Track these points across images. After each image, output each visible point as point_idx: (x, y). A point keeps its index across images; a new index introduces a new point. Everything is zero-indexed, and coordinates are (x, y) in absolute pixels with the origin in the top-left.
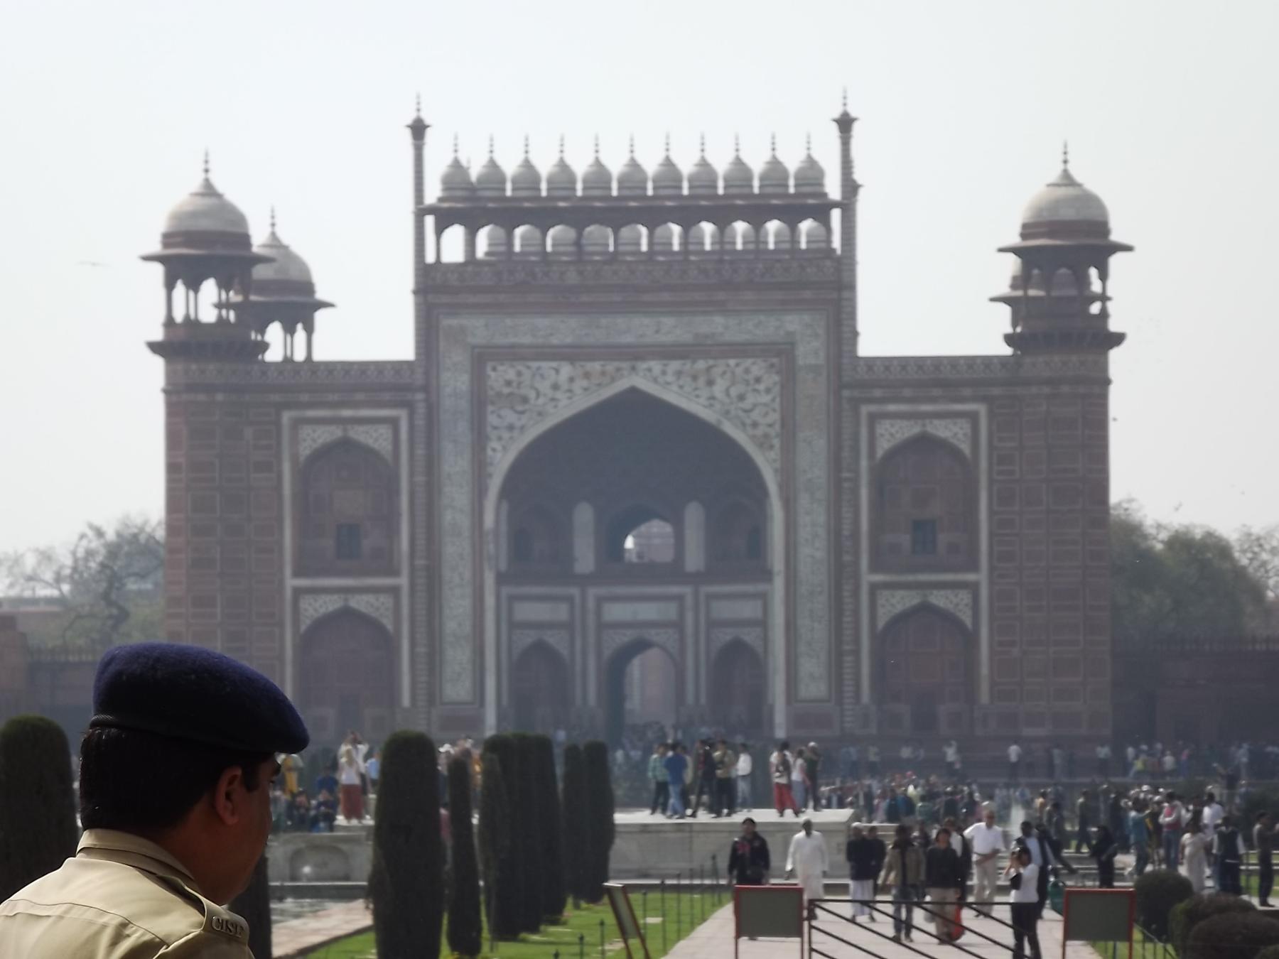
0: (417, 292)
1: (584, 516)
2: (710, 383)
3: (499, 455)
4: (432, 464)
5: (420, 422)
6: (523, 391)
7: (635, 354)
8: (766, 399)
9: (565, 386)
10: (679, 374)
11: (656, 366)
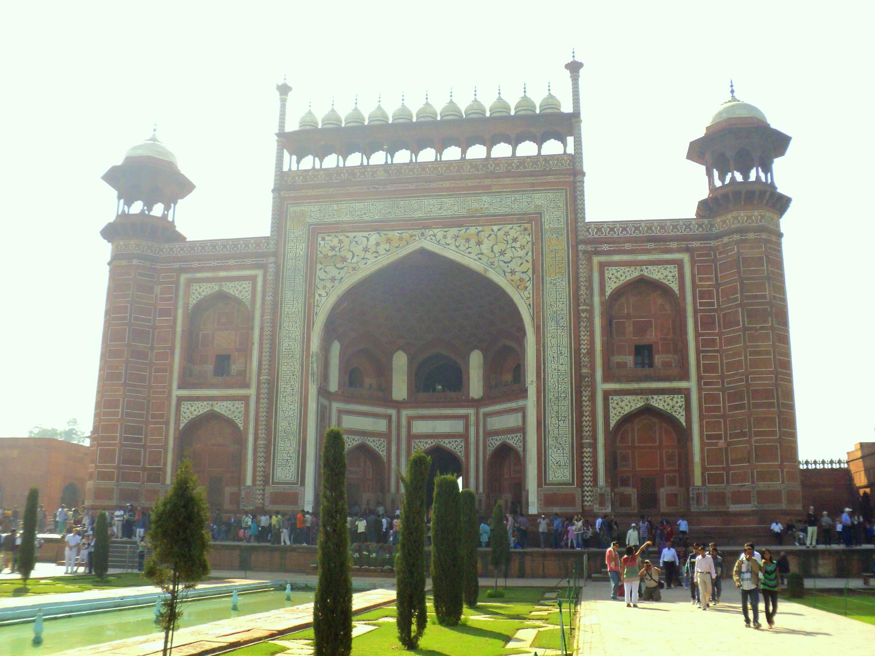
0: (273, 191)
1: (400, 361)
2: (479, 243)
3: (324, 299)
4: (276, 306)
5: (270, 278)
6: (342, 254)
7: (425, 225)
8: (521, 253)
10: (456, 238)
11: (439, 233)
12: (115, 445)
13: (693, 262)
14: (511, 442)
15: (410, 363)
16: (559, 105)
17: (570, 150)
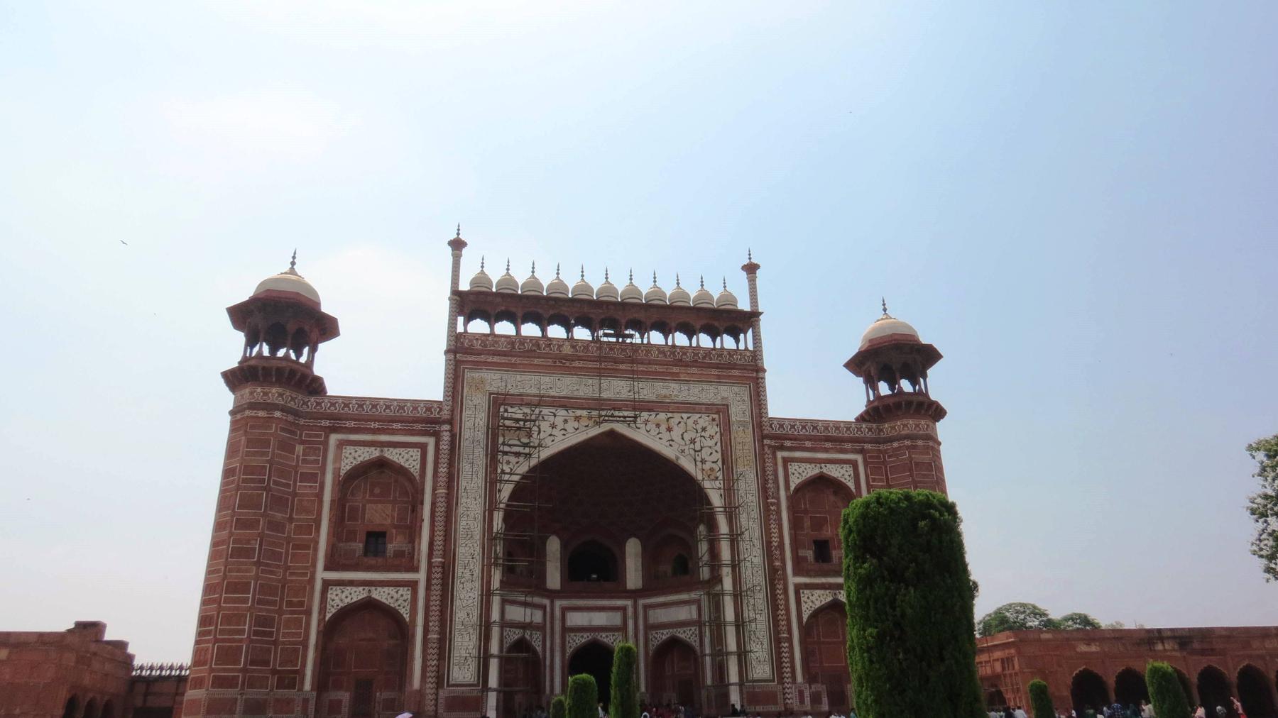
0: (447, 352)
1: (554, 546)
2: (669, 430)
4: (452, 479)
5: (445, 446)
8: (711, 443)
9: (561, 426)
12: (240, 641)
13: (866, 463)
14: (682, 636)
15: (564, 546)
16: (735, 300)
17: (751, 347)
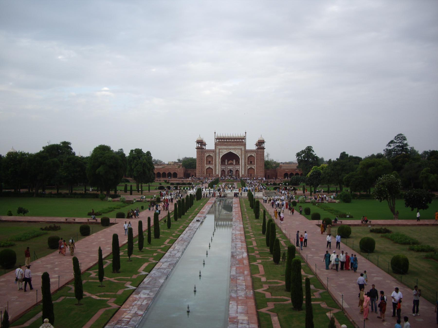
1: (226, 160)
4: (216, 157)
7: (230, 149)
